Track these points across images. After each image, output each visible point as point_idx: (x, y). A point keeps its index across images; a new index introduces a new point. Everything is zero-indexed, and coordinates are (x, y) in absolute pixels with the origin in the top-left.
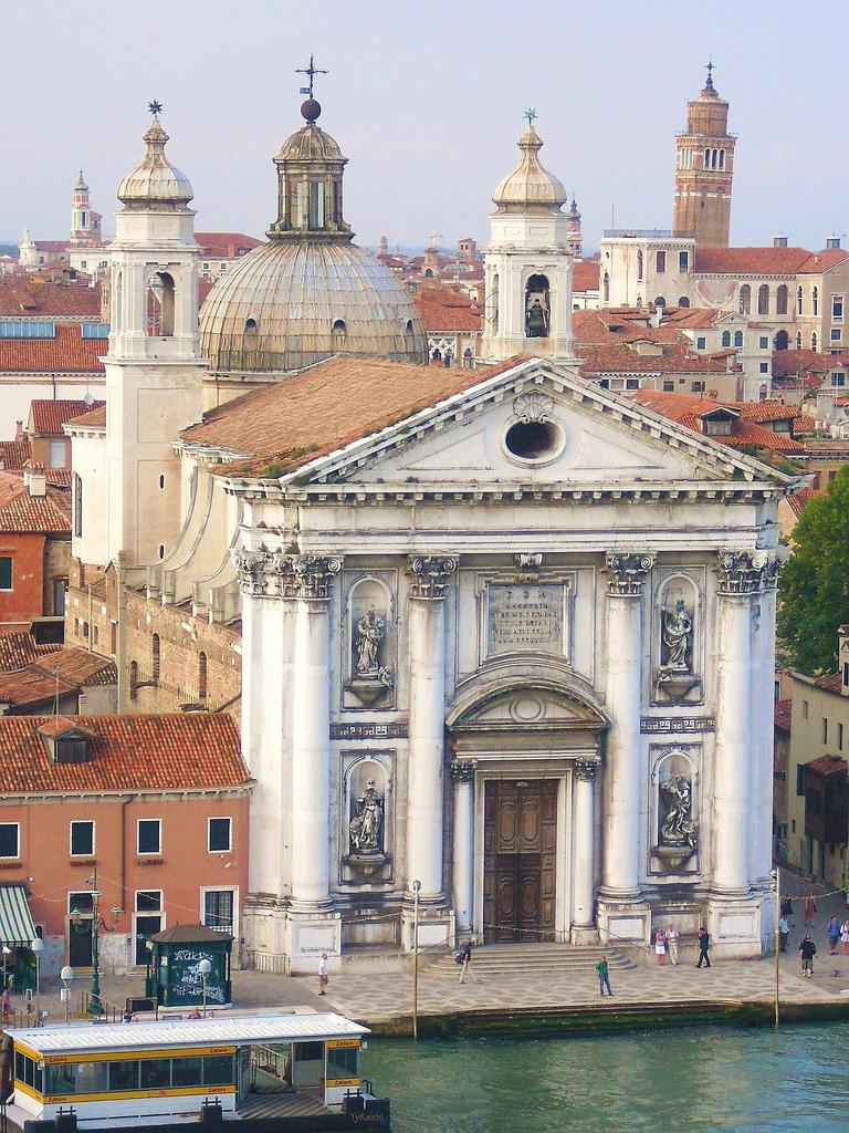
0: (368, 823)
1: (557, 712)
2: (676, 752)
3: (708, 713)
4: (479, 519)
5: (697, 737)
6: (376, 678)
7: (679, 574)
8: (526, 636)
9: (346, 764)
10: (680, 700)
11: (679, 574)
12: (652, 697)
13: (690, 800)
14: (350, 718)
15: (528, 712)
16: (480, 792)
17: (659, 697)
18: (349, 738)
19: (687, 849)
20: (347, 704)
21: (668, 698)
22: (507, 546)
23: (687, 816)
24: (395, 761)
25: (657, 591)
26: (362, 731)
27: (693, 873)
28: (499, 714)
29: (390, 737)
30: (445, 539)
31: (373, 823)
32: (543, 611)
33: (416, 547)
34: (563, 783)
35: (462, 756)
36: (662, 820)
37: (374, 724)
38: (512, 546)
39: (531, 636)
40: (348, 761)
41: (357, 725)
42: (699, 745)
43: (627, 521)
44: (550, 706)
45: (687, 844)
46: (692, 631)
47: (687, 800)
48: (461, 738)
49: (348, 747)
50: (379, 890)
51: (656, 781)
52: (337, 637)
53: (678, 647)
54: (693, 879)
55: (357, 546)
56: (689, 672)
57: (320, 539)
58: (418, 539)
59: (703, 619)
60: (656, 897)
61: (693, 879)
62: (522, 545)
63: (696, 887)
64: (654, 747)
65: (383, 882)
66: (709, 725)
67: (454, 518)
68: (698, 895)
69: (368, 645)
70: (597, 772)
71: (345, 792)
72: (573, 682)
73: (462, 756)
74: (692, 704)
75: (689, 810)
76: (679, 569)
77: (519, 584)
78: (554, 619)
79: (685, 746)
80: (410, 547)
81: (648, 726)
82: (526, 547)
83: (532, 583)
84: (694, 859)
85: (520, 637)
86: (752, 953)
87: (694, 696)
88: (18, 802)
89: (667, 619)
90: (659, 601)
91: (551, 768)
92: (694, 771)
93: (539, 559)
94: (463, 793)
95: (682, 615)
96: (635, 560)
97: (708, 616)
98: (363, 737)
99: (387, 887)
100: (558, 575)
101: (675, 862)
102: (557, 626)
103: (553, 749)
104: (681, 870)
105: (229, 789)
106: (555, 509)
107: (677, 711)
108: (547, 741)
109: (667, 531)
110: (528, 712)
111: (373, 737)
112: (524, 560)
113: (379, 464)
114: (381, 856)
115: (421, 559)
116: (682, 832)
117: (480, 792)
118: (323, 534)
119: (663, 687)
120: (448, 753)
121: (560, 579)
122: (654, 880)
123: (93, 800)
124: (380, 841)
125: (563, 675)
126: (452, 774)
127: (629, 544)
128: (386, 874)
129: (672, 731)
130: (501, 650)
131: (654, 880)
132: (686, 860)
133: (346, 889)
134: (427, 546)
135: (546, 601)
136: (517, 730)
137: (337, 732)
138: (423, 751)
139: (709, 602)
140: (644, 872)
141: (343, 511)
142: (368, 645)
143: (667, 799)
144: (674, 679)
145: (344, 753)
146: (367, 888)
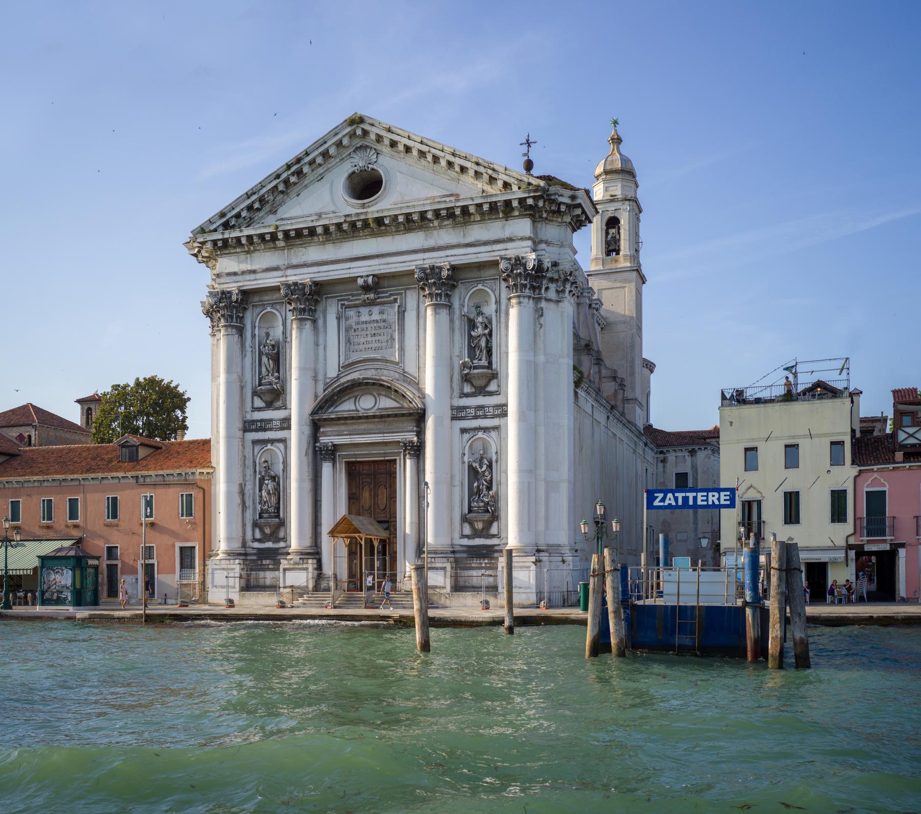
0: (264, 493)
1: (386, 403)
2: (480, 434)
3: (503, 402)
4: (330, 252)
5: (495, 422)
6: (270, 384)
7: (480, 286)
8: (370, 346)
9: (256, 451)
10: (481, 391)
11: (480, 286)
12: (462, 389)
13: (491, 473)
14: (258, 416)
15: (366, 404)
16: (340, 470)
17: (467, 389)
18: (256, 430)
19: (487, 516)
20: (256, 406)
21: (473, 390)
22: (348, 271)
23: (489, 488)
24: (286, 448)
25: (462, 299)
26: (264, 425)
27: (494, 536)
28: (347, 407)
29: (282, 429)
30: (306, 270)
31: (269, 493)
32: (382, 324)
33: (289, 278)
34: (398, 461)
35: (324, 440)
36: (471, 493)
37: (271, 420)
38: (352, 271)
39: (374, 345)
40: (257, 448)
41: (261, 421)
42: (496, 428)
43: (431, 243)
44: (383, 398)
45: (488, 511)
46: (490, 334)
47: (486, 474)
48: (324, 426)
49: (256, 438)
50: (276, 546)
51: (466, 459)
52: (249, 355)
53: (479, 347)
54: (494, 541)
55: (250, 283)
56: (490, 366)
57: (228, 279)
58: (289, 272)
59: (499, 321)
60: (465, 555)
61: (494, 541)
62: (358, 270)
63: (496, 548)
64: (463, 431)
65: (278, 540)
66: (502, 411)
67: (313, 253)
68: (496, 555)
69: (264, 359)
70: (417, 451)
71: (255, 472)
72: (404, 381)
73: (324, 440)
74: (491, 394)
75: (490, 482)
76: (479, 282)
77: (365, 304)
78: (390, 331)
79: (486, 430)
80: (284, 279)
81: (458, 414)
82: (363, 270)
83: (372, 303)
84: (495, 524)
85: (367, 346)
86: (526, 603)
87: (492, 387)
88: (77, 483)
89: (472, 325)
90: (466, 309)
91: (389, 450)
92: (494, 450)
93: (370, 280)
94: (327, 468)
95: (480, 319)
96: (434, 270)
97: (503, 320)
98: (265, 430)
99: (282, 544)
100: (391, 295)
101: (479, 526)
102: (392, 336)
103: (384, 433)
104: (485, 533)
105: (190, 471)
106: (380, 239)
107: (480, 400)
108: (381, 426)
109: (458, 246)
110: (366, 404)
111: (271, 429)
112: (360, 281)
113: (262, 217)
114: (277, 520)
115: (288, 286)
116: (483, 501)
117: (340, 470)
118: (229, 274)
119: (466, 379)
120: (315, 437)
121: (392, 298)
122: (465, 542)
123: (116, 481)
124: (278, 509)
125: (397, 376)
126: (319, 454)
127: (434, 261)
128: (281, 535)
129: (476, 417)
130: (355, 357)
131: (465, 542)
132: (489, 524)
133: (257, 545)
134: (293, 277)
135: (385, 317)
136: (356, 418)
137: (248, 426)
138: (295, 436)
139: (503, 307)
140: (457, 535)
141: (243, 256)
142: (264, 359)
143: (473, 473)
144: (476, 372)
145: (255, 442)
146: (269, 545)
